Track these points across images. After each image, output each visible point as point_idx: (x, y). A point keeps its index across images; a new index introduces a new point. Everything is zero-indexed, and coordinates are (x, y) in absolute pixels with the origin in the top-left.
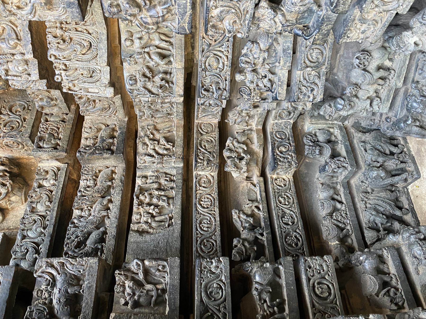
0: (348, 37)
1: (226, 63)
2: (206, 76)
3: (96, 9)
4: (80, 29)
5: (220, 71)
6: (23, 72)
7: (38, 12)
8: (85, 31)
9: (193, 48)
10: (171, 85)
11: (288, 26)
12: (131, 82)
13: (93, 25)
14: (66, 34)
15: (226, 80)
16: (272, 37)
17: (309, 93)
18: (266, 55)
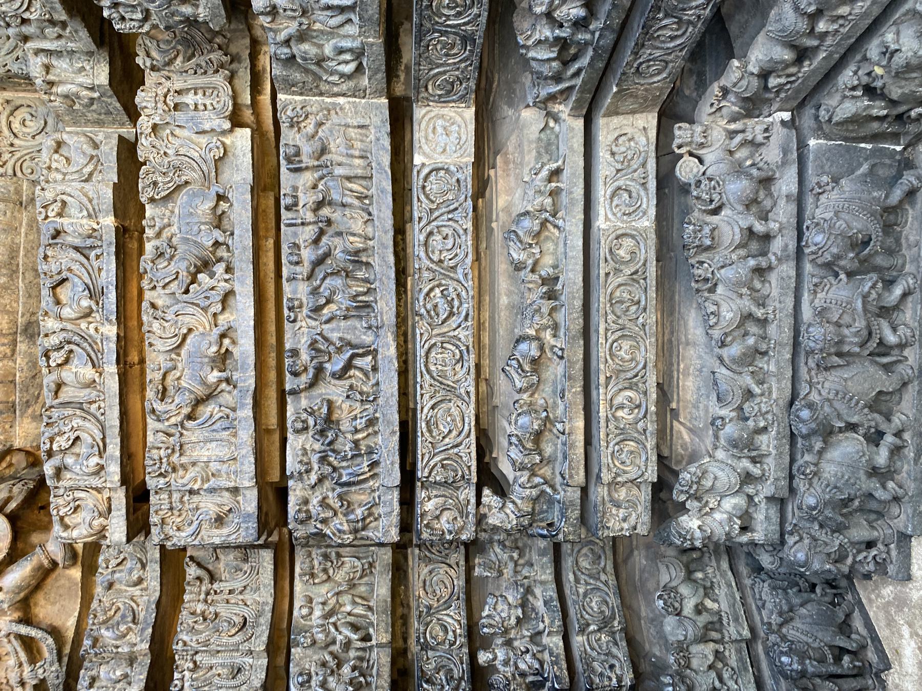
0: (608, 528)
1: (458, 631)
2: (428, 659)
3: (265, 564)
4: (233, 601)
5: (451, 645)
6: (120, 681)
7: (203, 533)
8: (240, 603)
9: (405, 640)
10: (369, 679)
11: (523, 516)
12: (300, 679)
13: (255, 592)
14: (212, 609)
15: (462, 663)
16: (522, 585)
17: (608, 672)
18: (519, 612)
